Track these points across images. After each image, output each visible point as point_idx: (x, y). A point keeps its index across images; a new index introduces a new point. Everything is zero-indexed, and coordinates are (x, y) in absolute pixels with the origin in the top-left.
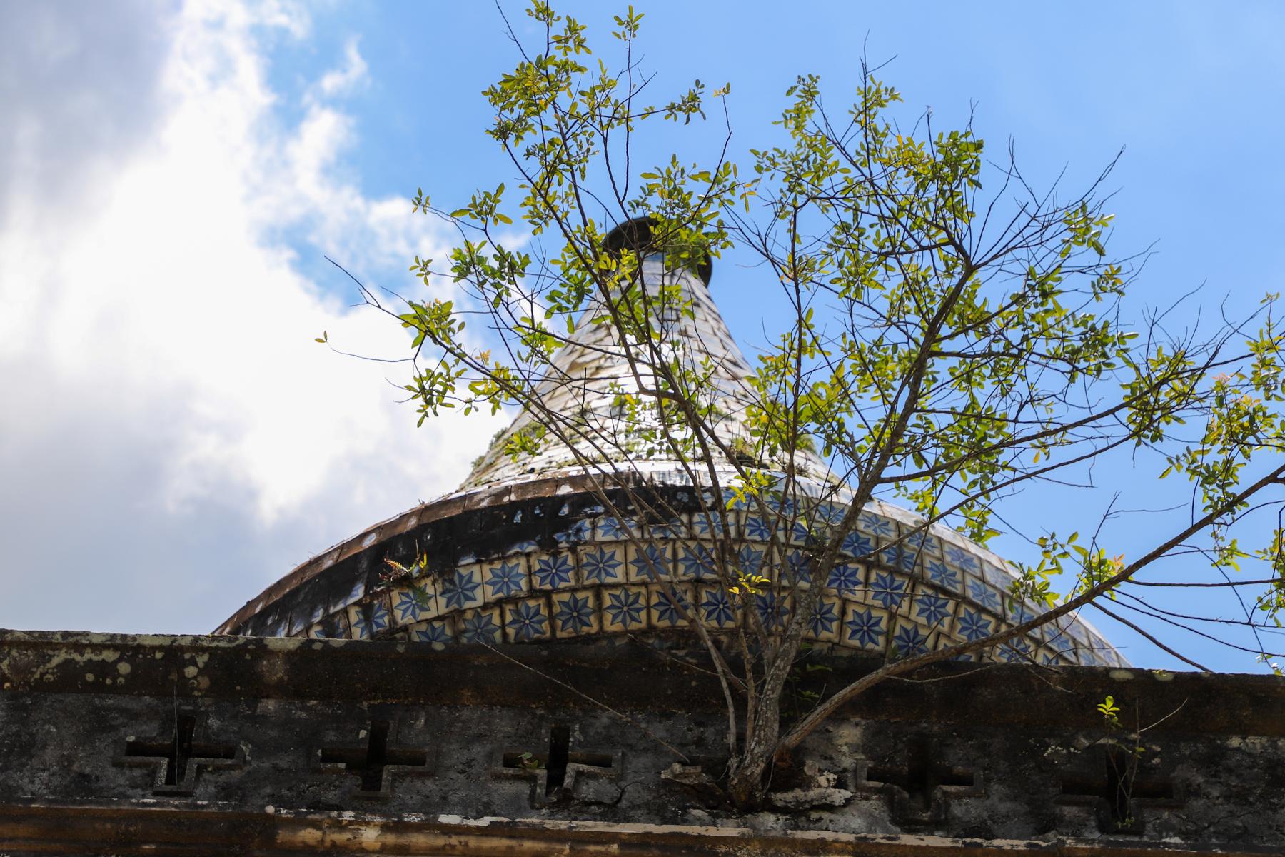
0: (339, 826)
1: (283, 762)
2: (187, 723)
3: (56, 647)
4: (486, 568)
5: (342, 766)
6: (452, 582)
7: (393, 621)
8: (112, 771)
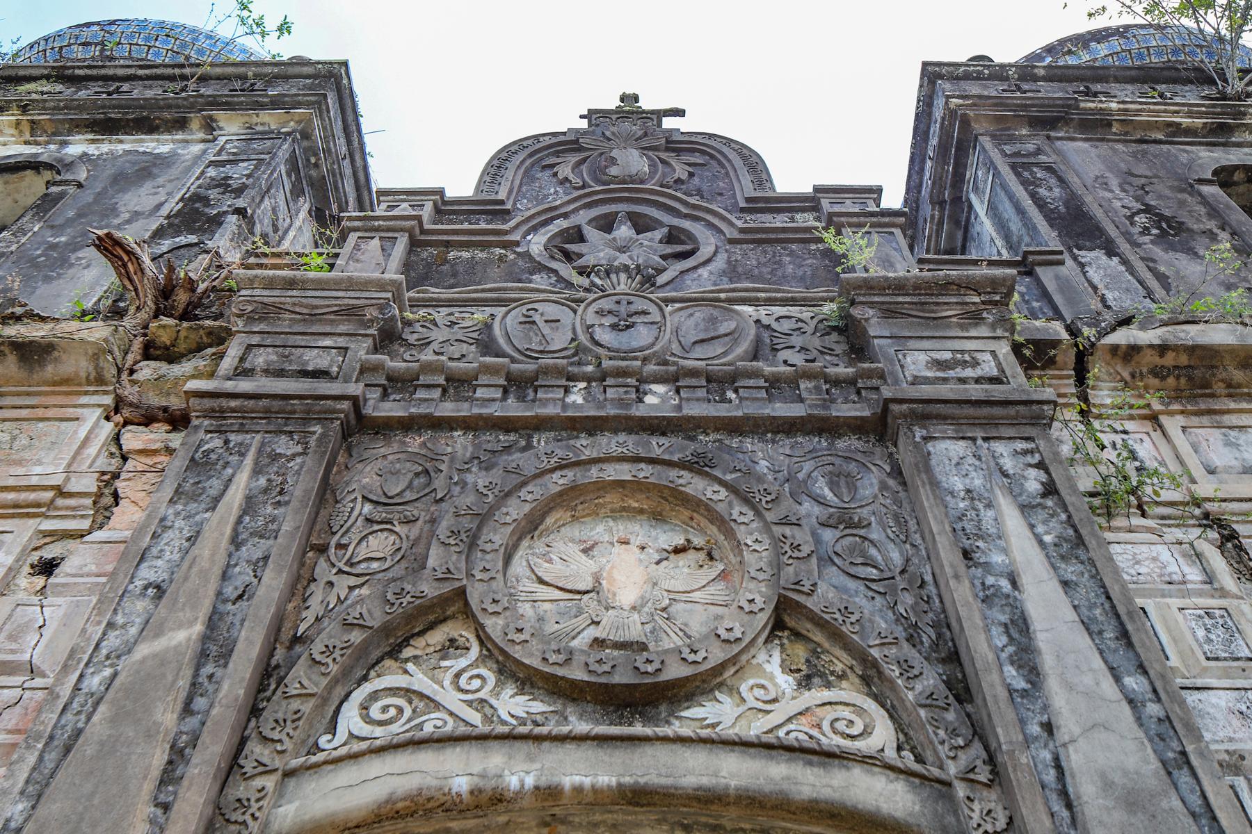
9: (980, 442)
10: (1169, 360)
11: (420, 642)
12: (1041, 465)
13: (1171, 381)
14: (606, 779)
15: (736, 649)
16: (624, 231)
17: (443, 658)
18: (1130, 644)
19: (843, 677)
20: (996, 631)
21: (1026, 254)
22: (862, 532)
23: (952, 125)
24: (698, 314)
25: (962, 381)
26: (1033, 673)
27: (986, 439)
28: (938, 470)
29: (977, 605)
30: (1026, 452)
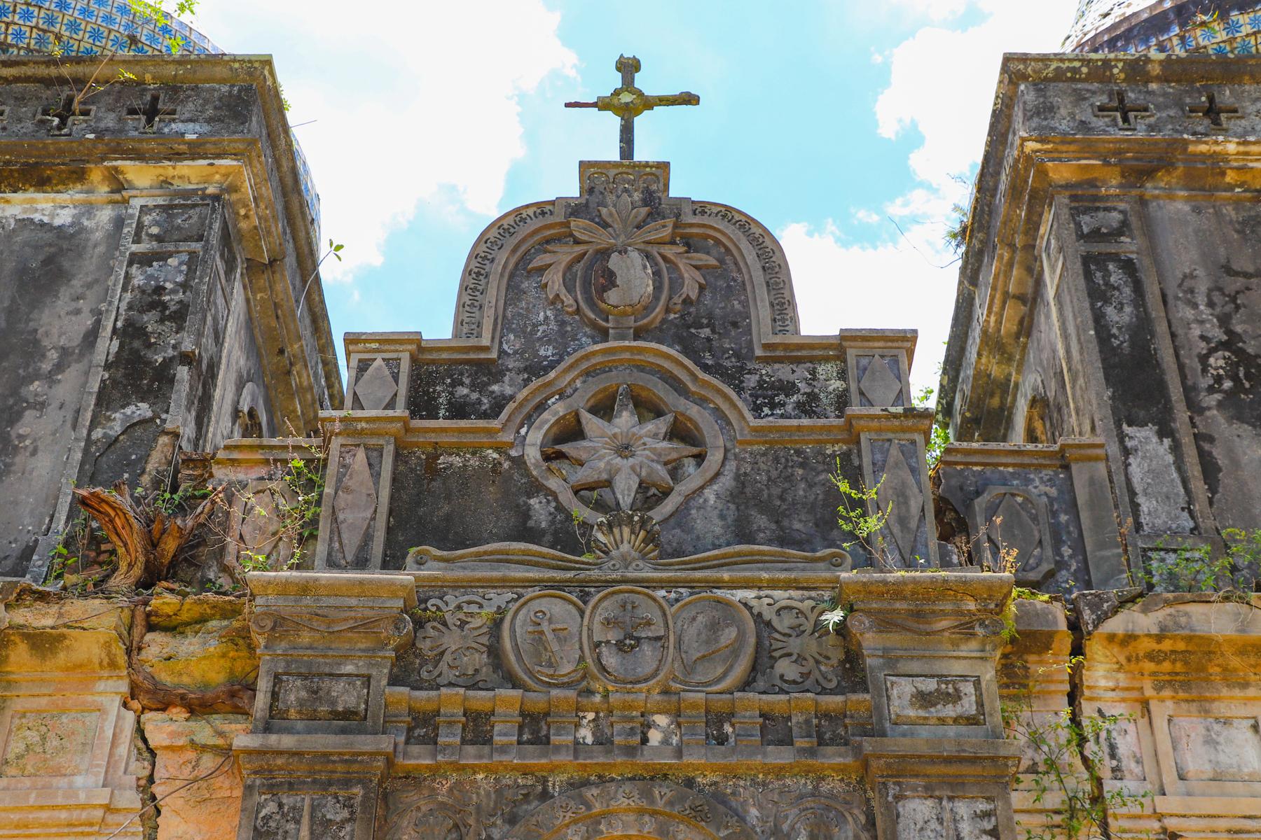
0: (1216, 143)
1: (1172, 113)
2: (1121, 96)
3: (1051, 60)
4: (1246, 16)
5: (1201, 114)
6: (1228, 23)
7: (1198, 43)
8: (1095, 119)
9: (944, 802)
10: (1167, 645)
16: (625, 420)
23: (1027, 170)
24: (700, 618)
25: (942, 721)
27: (951, 799)
30: (986, 815)
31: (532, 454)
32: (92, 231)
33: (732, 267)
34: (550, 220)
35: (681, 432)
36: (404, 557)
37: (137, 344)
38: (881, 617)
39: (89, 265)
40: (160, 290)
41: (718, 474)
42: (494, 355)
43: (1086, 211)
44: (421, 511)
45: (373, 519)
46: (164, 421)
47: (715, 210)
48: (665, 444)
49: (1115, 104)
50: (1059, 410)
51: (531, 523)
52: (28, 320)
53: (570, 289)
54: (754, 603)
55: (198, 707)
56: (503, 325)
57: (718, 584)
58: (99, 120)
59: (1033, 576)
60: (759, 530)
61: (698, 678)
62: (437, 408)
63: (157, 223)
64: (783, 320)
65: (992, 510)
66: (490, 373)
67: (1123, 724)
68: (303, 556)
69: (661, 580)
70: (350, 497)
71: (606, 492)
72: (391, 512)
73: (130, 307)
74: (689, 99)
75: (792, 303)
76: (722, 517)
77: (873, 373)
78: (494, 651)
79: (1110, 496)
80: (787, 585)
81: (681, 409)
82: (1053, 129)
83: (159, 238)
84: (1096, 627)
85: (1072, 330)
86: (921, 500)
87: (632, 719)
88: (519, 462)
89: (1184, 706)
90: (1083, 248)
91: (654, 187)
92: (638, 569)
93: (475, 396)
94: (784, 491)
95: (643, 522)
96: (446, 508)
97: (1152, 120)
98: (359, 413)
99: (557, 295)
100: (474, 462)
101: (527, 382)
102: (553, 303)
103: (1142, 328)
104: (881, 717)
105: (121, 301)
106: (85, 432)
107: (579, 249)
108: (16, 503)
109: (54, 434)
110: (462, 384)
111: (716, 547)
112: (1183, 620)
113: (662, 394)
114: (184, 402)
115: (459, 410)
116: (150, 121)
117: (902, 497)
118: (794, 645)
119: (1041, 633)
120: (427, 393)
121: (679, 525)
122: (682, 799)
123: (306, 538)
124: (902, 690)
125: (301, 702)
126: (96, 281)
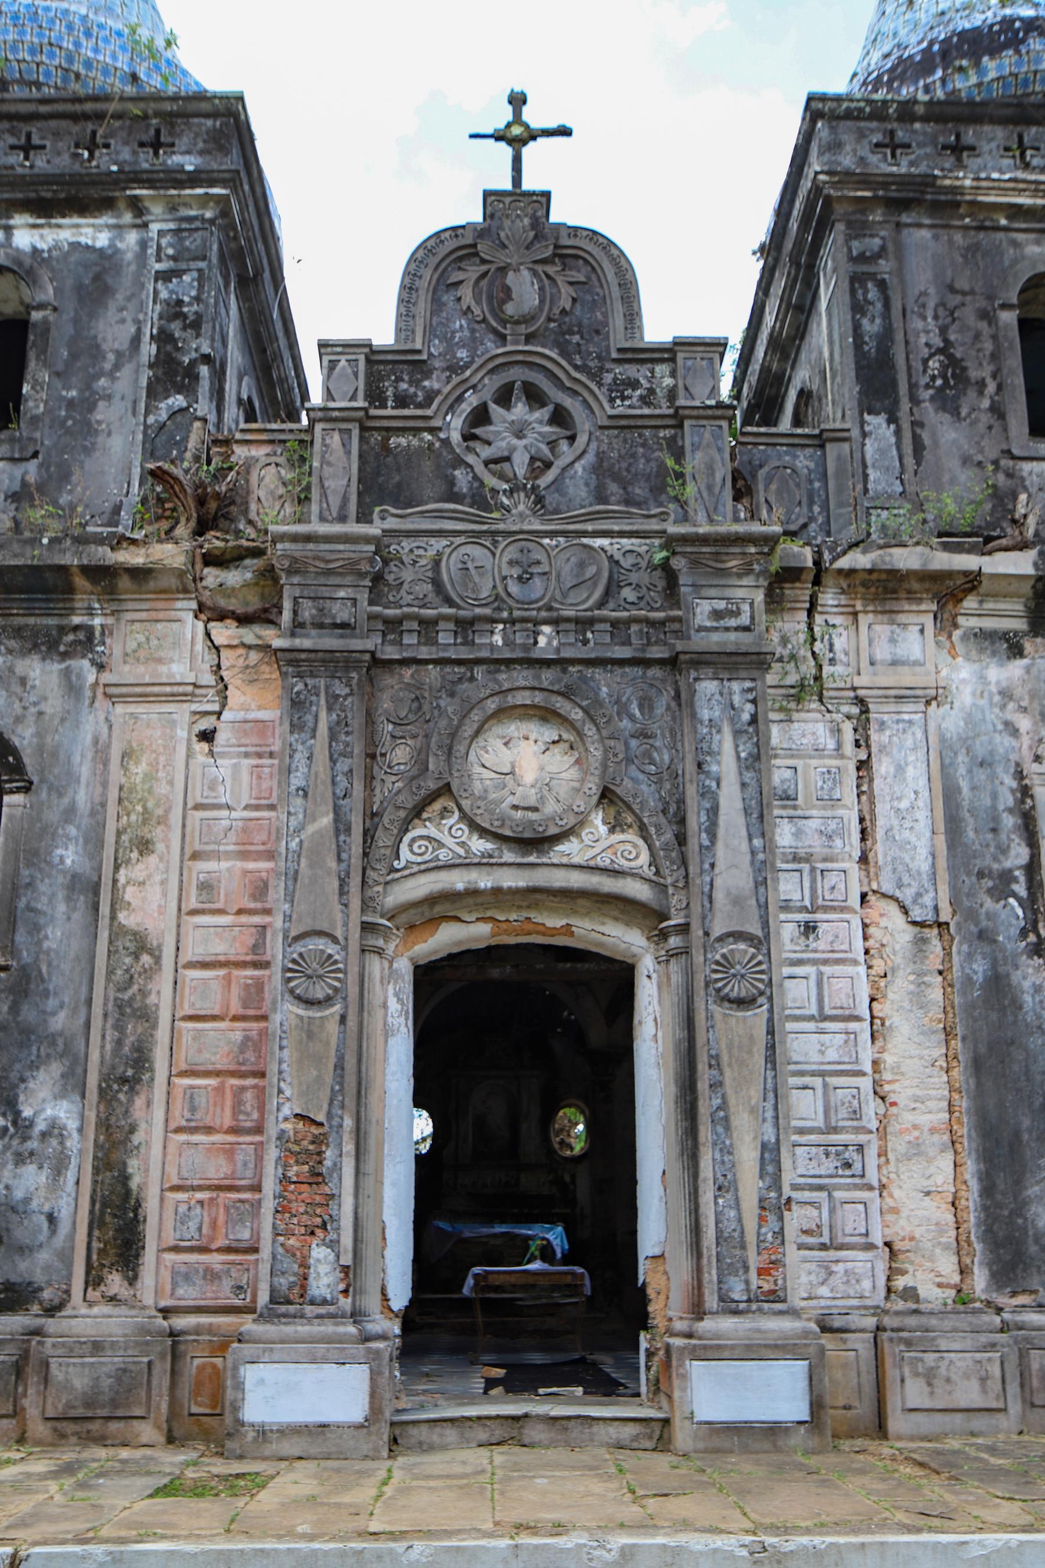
0: (957, 178)
2: (892, 133)
8: (870, 155)
11: (429, 809)
12: (754, 701)
13: (873, 590)
14: (522, 884)
15: (581, 817)
16: (520, 410)
17: (443, 818)
18: (762, 821)
19: (630, 826)
20: (703, 813)
21: (822, 431)
22: (651, 741)
24: (573, 559)
25: (727, 629)
26: (713, 836)
27: (729, 680)
28: (698, 704)
29: (696, 798)
30: (750, 690)
31: (456, 437)
32: (124, 252)
33: (597, 283)
34: (463, 242)
35: (560, 417)
36: (371, 513)
37: (169, 348)
38: (692, 557)
39: (126, 282)
40: (180, 303)
41: (584, 452)
42: (424, 357)
43: (856, 237)
44: (381, 479)
45: (348, 486)
46: (195, 410)
47: (585, 233)
48: (547, 429)
49: (887, 141)
50: (820, 400)
51: (456, 489)
52: (89, 329)
53: (478, 302)
54: (608, 548)
55: (244, 620)
56: (430, 332)
57: (585, 534)
58: (118, 153)
59: (793, 527)
60: (612, 494)
61: (570, 601)
62: (386, 399)
63: (171, 245)
64: (633, 328)
65: (769, 480)
66: (422, 372)
67: (841, 630)
68: (302, 513)
69: (546, 532)
70: (331, 470)
71: (506, 466)
72: (360, 481)
73: (161, 318)
74: (564, 132)
75: (639, 314)
76: (587, 484)
77: (695, 372)
78: (437, 584)
79: (850, 468)
80: (630, 534)
81: (559, 401)
82: (840, 164)
83: (174, 258)
84: (831, 564)
85: (836, 337)
86: (723, 471)
87: (527, 630)
88: (446, 442)
89: (880, 617)
90: (851, 267)
91: (539, 214)
92: (530, 523)
93: (412, 390)
94: (630, 465)
95: (533, 488)
96: (397, 478)
97: (913, 157)
98: (332, 405)
99: (469, 308)
100: (415, 442)
101: (449, 379)
102: (465, 313)
103: (886, 337)
104: (688, 628)
105: (153, 312)
106: (142, 419)
107: (484, 268)
108: (103, 473)
109: (121, 419)
110: (403, 380)
111: (582, 507)
112: (887, 559)
113: (545, 389)
114: (207, 395)
115: (402, 401)
116: (156, 154)
117: (711, 469)
118: (634, 577)
119: (796, 568)
120: (378, 387)
121: (557, 490)
122: (559, 681)
123: (303, 500)
124: (702, 611)
125: (313, 617)
126: (133, 295)
